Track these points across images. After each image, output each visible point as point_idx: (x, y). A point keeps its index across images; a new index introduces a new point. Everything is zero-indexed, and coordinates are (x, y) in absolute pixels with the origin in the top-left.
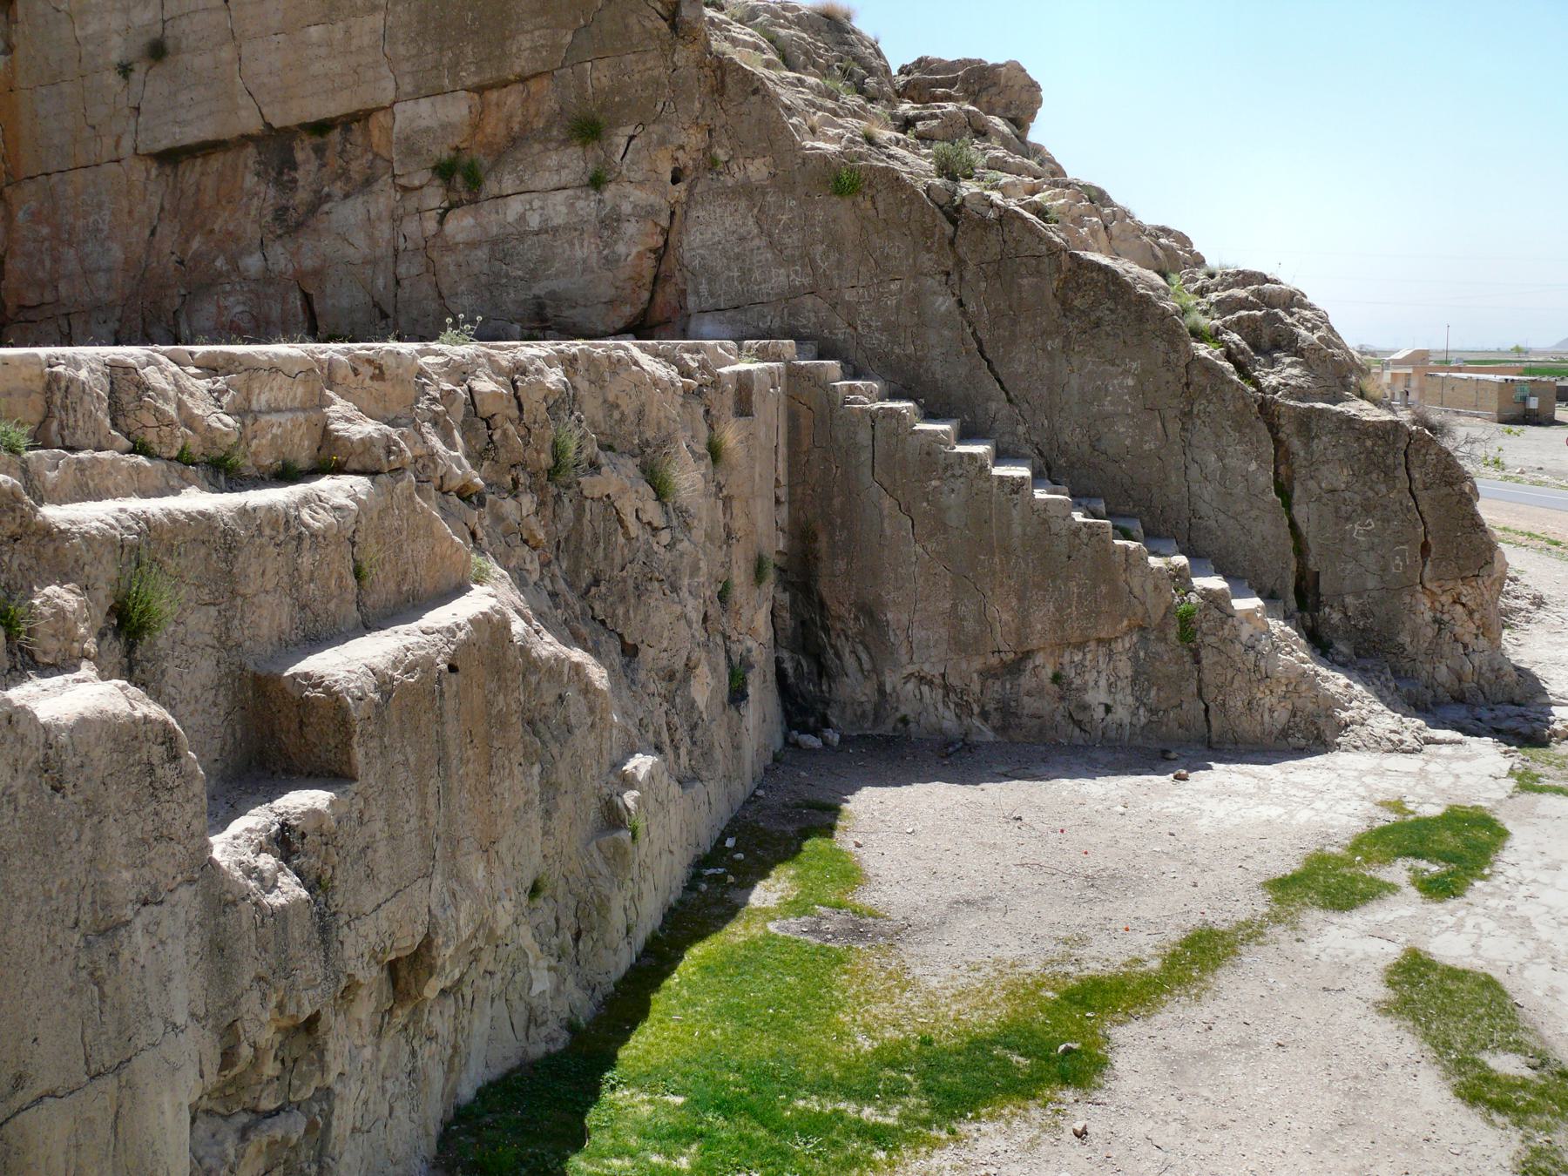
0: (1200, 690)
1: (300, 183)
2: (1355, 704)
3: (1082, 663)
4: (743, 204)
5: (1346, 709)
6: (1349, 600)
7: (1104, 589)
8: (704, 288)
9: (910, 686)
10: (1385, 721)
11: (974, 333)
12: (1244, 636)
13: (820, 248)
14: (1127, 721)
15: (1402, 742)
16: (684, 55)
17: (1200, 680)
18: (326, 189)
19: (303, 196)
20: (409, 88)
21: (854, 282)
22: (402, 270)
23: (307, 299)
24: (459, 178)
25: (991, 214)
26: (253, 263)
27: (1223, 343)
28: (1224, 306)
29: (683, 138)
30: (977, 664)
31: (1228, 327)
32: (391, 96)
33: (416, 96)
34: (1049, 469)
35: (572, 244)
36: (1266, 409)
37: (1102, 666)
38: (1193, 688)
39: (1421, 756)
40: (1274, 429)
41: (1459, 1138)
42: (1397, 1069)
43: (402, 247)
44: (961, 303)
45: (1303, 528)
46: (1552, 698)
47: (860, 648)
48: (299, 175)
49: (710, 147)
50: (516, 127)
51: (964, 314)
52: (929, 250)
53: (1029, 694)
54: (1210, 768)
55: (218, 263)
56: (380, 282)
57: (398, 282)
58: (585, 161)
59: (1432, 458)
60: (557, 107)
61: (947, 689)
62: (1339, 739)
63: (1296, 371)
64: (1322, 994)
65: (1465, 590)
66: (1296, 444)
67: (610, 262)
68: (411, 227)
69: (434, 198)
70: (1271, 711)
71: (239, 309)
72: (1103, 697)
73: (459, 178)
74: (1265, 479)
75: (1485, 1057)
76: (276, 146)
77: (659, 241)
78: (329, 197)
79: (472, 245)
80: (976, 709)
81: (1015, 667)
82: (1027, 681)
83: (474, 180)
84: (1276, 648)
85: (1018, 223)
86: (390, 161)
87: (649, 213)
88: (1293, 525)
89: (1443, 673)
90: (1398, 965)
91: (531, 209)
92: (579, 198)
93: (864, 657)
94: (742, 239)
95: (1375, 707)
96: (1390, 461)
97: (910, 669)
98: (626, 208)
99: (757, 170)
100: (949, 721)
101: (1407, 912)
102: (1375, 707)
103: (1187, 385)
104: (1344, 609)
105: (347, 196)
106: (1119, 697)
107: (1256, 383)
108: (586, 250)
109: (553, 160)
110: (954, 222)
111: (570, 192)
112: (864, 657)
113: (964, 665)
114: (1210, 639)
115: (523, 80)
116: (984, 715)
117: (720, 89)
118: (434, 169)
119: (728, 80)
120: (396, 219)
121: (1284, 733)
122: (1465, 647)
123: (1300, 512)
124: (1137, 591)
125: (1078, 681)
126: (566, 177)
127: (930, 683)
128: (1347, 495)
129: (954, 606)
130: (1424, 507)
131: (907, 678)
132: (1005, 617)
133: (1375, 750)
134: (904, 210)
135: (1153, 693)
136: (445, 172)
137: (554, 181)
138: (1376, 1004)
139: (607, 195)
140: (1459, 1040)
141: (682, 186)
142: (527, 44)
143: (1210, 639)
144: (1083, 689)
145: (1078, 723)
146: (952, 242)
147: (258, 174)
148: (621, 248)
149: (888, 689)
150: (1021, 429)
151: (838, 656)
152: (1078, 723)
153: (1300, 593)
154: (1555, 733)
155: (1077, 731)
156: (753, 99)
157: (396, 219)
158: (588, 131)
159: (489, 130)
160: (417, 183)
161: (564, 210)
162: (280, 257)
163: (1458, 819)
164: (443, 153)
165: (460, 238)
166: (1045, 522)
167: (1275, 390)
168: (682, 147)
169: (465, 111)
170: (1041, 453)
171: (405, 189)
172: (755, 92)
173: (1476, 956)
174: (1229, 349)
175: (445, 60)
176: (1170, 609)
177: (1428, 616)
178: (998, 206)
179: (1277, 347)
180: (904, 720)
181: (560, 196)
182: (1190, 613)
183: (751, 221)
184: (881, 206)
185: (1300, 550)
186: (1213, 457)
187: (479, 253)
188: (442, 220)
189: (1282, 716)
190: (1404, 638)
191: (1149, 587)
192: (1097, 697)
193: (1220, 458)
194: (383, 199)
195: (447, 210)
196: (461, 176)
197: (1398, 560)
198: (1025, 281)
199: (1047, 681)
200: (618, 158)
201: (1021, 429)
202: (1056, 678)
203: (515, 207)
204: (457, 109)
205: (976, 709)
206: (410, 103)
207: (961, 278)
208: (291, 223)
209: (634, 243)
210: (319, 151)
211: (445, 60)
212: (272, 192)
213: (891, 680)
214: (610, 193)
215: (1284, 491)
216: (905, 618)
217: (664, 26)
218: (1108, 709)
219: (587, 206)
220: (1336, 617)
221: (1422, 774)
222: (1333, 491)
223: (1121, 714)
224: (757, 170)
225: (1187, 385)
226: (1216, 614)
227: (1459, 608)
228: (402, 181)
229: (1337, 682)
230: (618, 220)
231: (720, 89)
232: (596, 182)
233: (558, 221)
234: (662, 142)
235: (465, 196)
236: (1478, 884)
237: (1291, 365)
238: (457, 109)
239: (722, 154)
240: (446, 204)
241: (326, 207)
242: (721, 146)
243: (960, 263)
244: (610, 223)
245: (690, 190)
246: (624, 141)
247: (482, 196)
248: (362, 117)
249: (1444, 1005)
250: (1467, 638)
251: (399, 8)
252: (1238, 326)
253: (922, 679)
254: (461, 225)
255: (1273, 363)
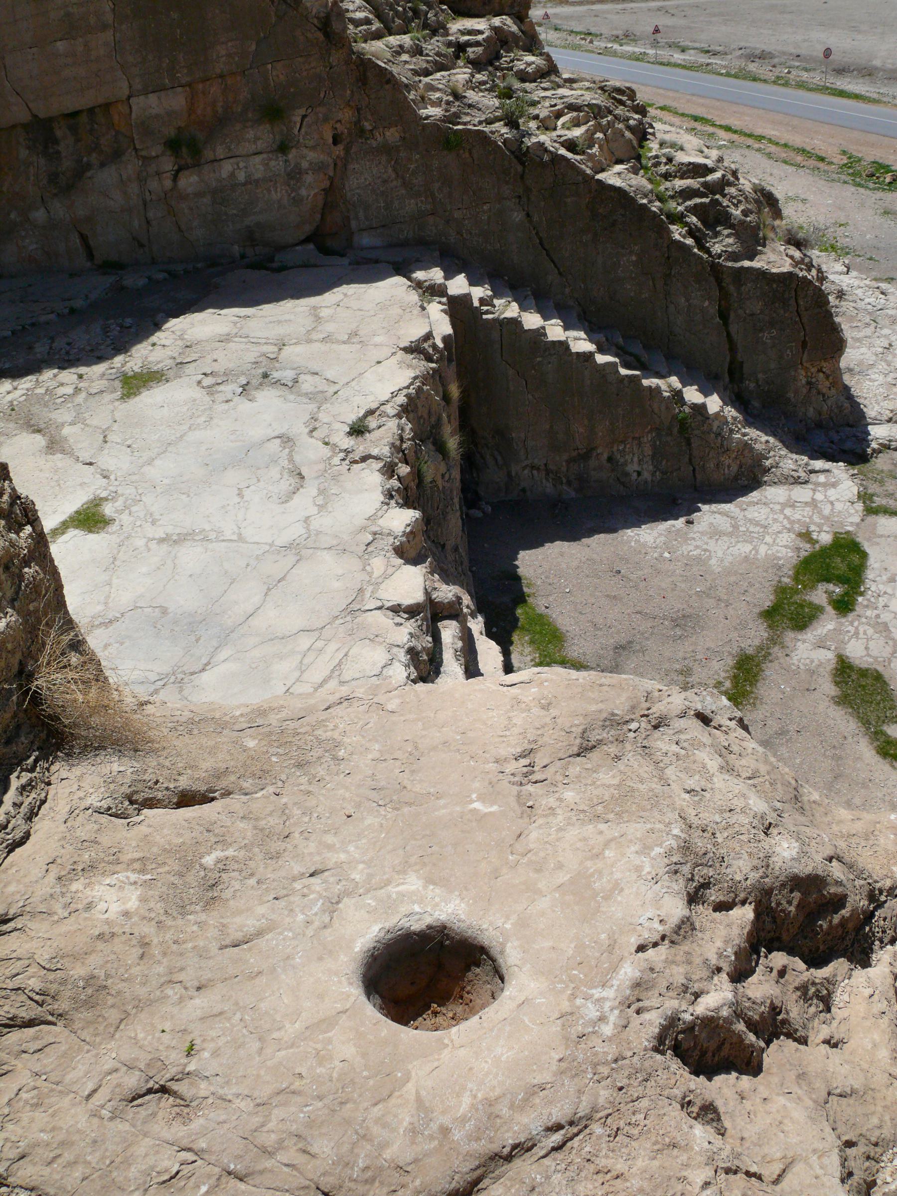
0: (690, 459)
1: (64, 154)
2: (772, 453)
3: (624, 450)
4: (384, 159)
5: (767, 459)
6: (760, 376)
7: (637, 410)
8: (361, 215)
9: (526, 472)
10: (790, 461)
11: (537, 234)
12: (715, 429)
13: (437, 185)
14: (649, 479)
15: (799, 477)
16: (336, 57)
17: (691, 455)
18: (85, 159)
19: (67, 164)
20: (140, 87)
21: (460, 206)
22: (151, 215)
23: (84, 238)
24: (184, 150)
25: (546, 158)
26: (39, 215)
27: (686, 224)
28: (687, 194)
29: (340, 116)
30: (565, 457)
31: (689, 210)
32: (127, 92)
33: (146, 92)
34: (585, 313)
35: (269, 191)
36: (716, 270)
37: (635, 450)
38: (687, 460)
39: (810, 486)
40: (719, 281)
41: (882, 777)
42: (850, 739)
43: (148, 198)
44: (528, 215)
45: (735, 337)
46: (869, 421)
47: (496, 453)
48: (61, 148)
49: (359, 121)
50: (220, 110)
51: (531, 222)
52: (507, 183)
53: (594, 470)
54: (699, 510)
55: (12, 216)
56: (136, 223)
57: (148, 222)
58: (273, 133)
59: (810, 292)
60: (249, 96)
61: (548, 472)
62: (766, 479)
63: (731, 240)
64: (807, 693)
65: (824, 364)
66: (732, 289)
67: (297, 201)
68: (153, 184)
69: (168, 164)
70: (729, 466)
71: (35, 246)
72: (636, 467)
73: (184, 150)
74: (713, 310)
75: (885, 728)
76: (41, 131)
77: (327, 184)
78: (89, 166)
79: (199, 195)
80: (564, 480)
81: (586, 456)
82: (593, 463)
83: (195, 150)
84: (731, 431)
85: (564, 163)
86: (133, 140)
87: (319, 168)
88: (729, 335)
89: (811, 412)
90: (836, 669)
91: (238, 168)
92: (271, 159)
93: (499, 458)
94: (385, 181)
95: (782, 453)
96: (786, 296)
97: (526, 463)
98: (305, 165)
99: (392, 135)
100: (549, 487)
101: (831, 626)
102: (782, 453)
103: (668, 258)
104: (757, 381)
105: (102, 165)
106: (645, 466)
107: (707, 251)
108: (278, 194)
109: (250, 134)
110: (522, 163)
111: (265, 156)
112: (499, 458)
113: (558, 458)
114: (696, 432)
115: (221, 76)
116: (569, 483)
117: (363, 80)
118: (165, 144)
119: (369, 74)
120: (142, 180)
121: (736, 478)
122: (824, 395)
123: (733, 328)
124: (656, 410)
125: (622, 460)
126: (261, 145)
127: (538, 469)
128: (761, 316)
129: (551, 427)
130: (805, 320)
131: (524, 468)
132: (581, 430)
133: (785, 484)
134: (491, 157)
135: (664, 462)
136: (173, 145)
137: (253, 148)
138: (833, 698)
139: (290, 156)
140: (873, 718)
141: (341, 147)
142: (223, 52)
143: (696, 432)
144: (625, 464)
145: (623, 484)
146: (522, 177)
147: (28, 148)
148: (303, 192)
149: (513, 474)
150: (567, 290)
151: (482, 457)
152: (623, 484)
153: (731, 372)
154: (874, 450)
155: (622, 488)
156: (387, 87)
157: (142, 180)
158: (273, 112)
159: (199, 112)
160: (154, 154)
161: (261, 168)
162: (59, 209)
163: (841, 546)
164: (170, 132)
165: (190, 190)
166: (604, 376)
167: (720, 256)
168: (340, 121)
169: (183, 102)
170: (579, 304)
171: (144, 158)
172: (388, 82)
173: (868, 655)
174: (690, 228)
175: (164, 65)
176: (674, 417)
177: (804, 381)
178: (551, 152)
179: (718, 222)
180: (524, 490)
181: (258, 159)
182: (684, 419)
183: (390, 170)
184: (475, 156)
185: (733, 349)
186: (683, 300)
187: (205, 200)
188: (175, 178)
189: (735, 468)
190: (791, 395)
191: (663, 408)
192: (632, 468)
193: (687, 300)
194: (130, 166)
195: (178, 172)
196: (186, 147)
197: (788, 352)
198: (569, 200)
199: (605, 462)
200: (296, 131)
201: (567, 290)
202: (610, 459)
203: (227, 168)
204: (177, 101)
205: (564, 480)
206: (142, 98)
207: (529, 200)
208: (66, 184)
209: (311, 188)
210: (74, 129)
211: (164, 65)
212: (42, 161)
213: (515, 469)
214: (292, 155)
215: (724, 315)
216: (522, 435)
217: (320, 36)
218: (639, 474)
219: (278, 164)
220: (752, 385)
221: (813, 504)
222: (752, 315)
223: (646, 475)
224: (392, 135)
225: (668, 258)
226: (699, 418)
227: (821, 375)
228: (143, 153)
229: (760, 439)
230: (300, 173)
231: (363, 80)
232: (283, 148)
233: (258, 175)
234: (326, 119)
235: (189, 161)
236: (860, 599)
237: (728, 236)
238: (177, 101)
239: (367, 126)
240: (176, 168)
241: (89, 174)
242: (367, 120)
243: (528, 190)
244: (295, 175)
245: (347, 150)
246: (299, 119)
247: (203, 161)
248: (107, 106)
249: (856, 684)
250: (824, 390)
251: (124, 27)
252: (694, 210)
253: (533, 467)
254: (189, 182)
255: (716, 234)
